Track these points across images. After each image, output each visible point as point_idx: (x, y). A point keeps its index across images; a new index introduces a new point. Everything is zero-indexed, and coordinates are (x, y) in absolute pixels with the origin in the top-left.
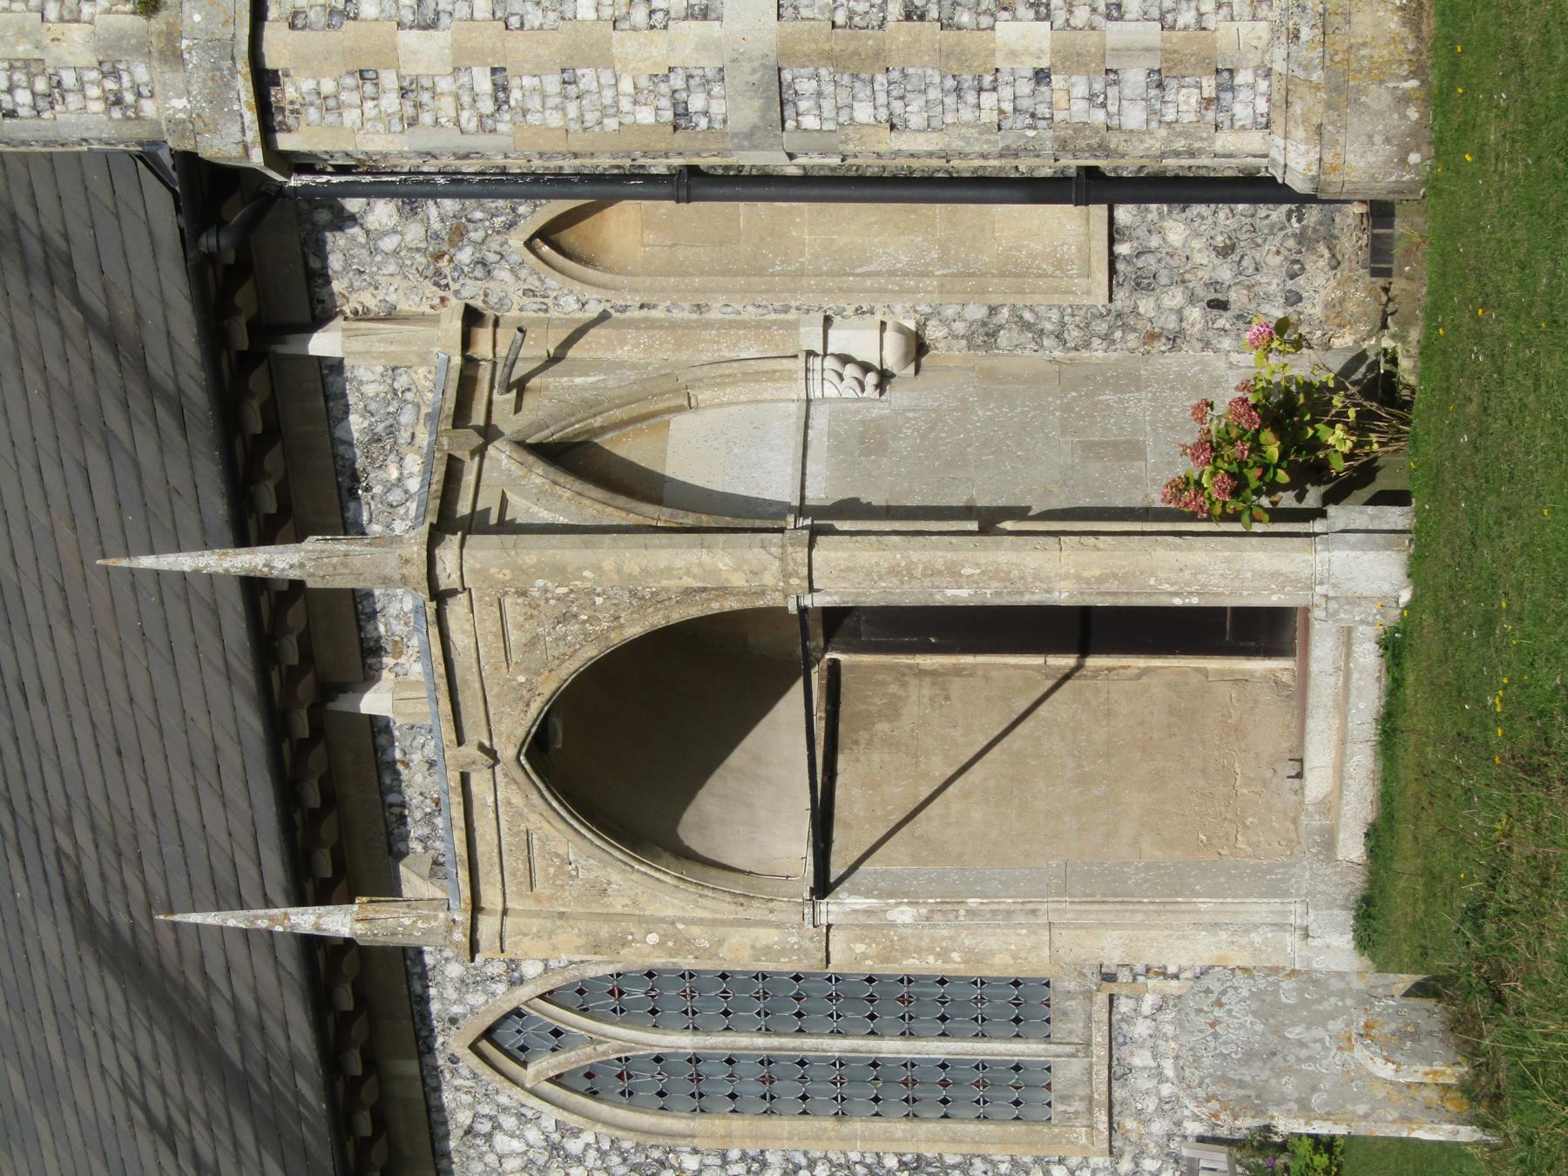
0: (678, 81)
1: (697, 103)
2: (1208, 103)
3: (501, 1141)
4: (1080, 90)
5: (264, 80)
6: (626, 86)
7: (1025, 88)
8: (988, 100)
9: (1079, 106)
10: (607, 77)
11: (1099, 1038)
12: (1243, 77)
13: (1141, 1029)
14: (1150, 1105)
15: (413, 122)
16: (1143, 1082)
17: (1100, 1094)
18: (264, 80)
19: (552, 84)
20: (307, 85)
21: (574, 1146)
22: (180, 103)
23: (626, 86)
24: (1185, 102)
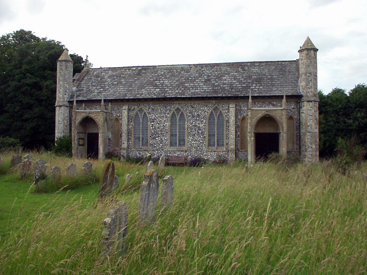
1: (309, 127)
12: (312, 160)
14: (212, 153)
15: (308, 110)
19: (311, 118)
23: (311, 123)
24: (310, 156)
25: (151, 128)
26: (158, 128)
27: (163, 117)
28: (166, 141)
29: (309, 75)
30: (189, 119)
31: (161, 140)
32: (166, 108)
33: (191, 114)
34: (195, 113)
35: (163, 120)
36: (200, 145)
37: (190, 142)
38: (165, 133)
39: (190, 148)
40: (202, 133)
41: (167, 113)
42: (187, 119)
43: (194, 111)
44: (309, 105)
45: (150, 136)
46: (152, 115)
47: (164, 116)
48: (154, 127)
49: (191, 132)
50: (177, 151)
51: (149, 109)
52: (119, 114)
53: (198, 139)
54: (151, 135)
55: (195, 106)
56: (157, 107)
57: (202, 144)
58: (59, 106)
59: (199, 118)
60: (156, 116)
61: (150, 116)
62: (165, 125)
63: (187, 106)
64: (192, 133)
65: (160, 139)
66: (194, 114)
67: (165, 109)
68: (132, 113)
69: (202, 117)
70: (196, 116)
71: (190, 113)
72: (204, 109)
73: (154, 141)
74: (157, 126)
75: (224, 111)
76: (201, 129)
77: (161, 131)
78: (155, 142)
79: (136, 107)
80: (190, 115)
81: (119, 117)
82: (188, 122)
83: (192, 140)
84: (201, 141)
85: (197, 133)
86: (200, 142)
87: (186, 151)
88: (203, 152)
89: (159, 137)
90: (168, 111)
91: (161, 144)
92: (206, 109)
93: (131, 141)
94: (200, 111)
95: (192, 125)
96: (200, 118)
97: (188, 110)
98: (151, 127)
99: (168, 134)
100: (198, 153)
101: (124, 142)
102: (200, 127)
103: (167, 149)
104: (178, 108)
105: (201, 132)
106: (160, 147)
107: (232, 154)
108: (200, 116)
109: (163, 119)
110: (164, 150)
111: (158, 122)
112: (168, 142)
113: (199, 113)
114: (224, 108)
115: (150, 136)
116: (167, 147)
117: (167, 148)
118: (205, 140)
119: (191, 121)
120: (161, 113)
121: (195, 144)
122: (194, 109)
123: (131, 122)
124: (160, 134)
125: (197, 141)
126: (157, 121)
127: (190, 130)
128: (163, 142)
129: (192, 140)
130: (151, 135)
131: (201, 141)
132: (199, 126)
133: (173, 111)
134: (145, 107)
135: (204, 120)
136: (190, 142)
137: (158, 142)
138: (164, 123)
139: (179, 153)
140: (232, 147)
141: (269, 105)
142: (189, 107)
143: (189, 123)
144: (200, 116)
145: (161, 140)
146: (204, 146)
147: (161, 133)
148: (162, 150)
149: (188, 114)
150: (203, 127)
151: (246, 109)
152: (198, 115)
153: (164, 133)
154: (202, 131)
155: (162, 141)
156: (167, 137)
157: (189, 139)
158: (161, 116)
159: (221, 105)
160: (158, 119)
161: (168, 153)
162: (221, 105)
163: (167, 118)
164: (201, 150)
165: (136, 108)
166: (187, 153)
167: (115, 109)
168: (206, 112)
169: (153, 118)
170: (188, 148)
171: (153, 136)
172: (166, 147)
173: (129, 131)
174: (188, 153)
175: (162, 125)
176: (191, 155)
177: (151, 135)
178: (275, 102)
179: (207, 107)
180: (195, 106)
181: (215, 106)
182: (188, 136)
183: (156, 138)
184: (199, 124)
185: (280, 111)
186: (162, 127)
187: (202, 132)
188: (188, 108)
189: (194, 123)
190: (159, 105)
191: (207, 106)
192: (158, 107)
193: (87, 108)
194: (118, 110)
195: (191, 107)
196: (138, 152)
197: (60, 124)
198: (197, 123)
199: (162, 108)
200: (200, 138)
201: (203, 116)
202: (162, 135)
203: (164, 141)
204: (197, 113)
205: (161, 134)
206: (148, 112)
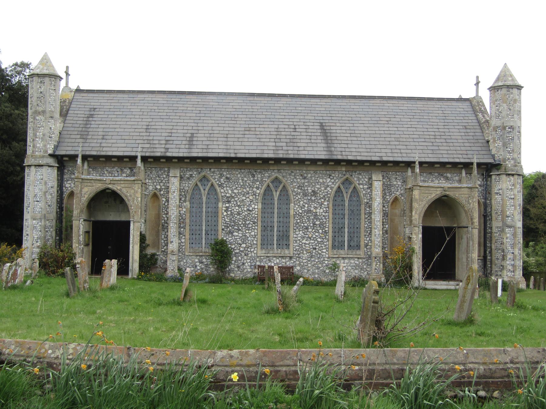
0: (512, 217)
1: (509, 218)
2: (510, 270)
4: (511, 257)
5: (513, 175)
6: (512, 211)
7: (511, 251)
8: (510, 248)
9: (509, 257)
10: (513, 209)
11: (349, 256)
12: (513, 273)
13: (353, 261)
16: (342, 261)
17: (340, 256)
18: (513, 175)
19: (512, 204)
20: (512, 179)
22: (509, 166)
23: (512, 211)
24: (510, 268)
26: (239, 214)
27: (248, 193)
28: (252, 239)
29: (509, 130)
30: (297, 198)
31: (243, 237)
32: (254, 177)
33: (301, 189)
34: (309, 188)
35: (248, 199)
36: (317, 247)
37: (298, 242)
38: (251, 223)
39: (298, 252)
40: (322, 225)
41: (255, 186)
42: (294, 199)
43: (306, 184)
44: (510, 181)
45: (223, 229)
46: (227, 190)
47: (250, 191)
48: (229, 213)
49: (300, 222)
50: (275, 257)
51: (221, 177)
52: (159, 185)
53: (314, 236)
54: (225, 226)
55: (309, 175)
56: (237, 174)
57: (321, 244)
58: (35, 166)
59: (315, 197)
60: (235, 191)
61: (222, 191)
62: (251, 209)
63: (293, 174)
64: (302, 225)
65: (241, 235)
66: (307, 190)
67: (252, 179)
68: (187, 185)
69: (321, 196)
70: (310, 194)
71: (298, 188)
72: (325, 181)
73: (230, 239)
74: (235, 210)
75: (361, 186)
76: (320, 217)
77: (245, 220)
78: (232, 241)
79: (195, 173)
80: (299, 191)
81: (160, 191)
82: (295, 204)
83: (303, 238)
84: (319, 240)
85: (311, 225)
86: (318, 241)
87: (291, 258)
88: (322, 259)
89: (240, 230)
90: (258, 183)
91: (244, 243)
92: (328, 181)
93: (183, 237)
94: (318, 185)
95: (303, 210)
96: (318, 198)
97: (295, 182)
98: (223, 211)
99: (257, 226)
101: (172, 240)
102: (318, 214)
103: (255, 253)
104: (276, 178)
105: (319, 222)
106: (241, 249)
107: (379, 264)
108: (318, 193)
109: (248, 198)
110: (250, 255)
111: (239, 204)
112: (257, 241)
113: (316, 189)
114: (361, 182)
115: (223, 229)
116: (256, 249)
117: (255, 252)
118: (327, 237)
119: (302, 203)
120: (243, 187)
121: (308, 244)
122: (306, 181)
123: (185, 201)
124: (242, 226)
125: (312, 239)
126: (236, 201)
127: (300, 219)
128: (248, 240)
129: (303, 238)
130: (223, 227)
131: (319, 240)
132: (317, 213)
133: (267, 183)
134: (212, 174)
135: (324, 202)
136: (299, 240)
137: (238, 240)
138: (250, 205)
139: (278, 261)
140: (377, 250)
141: (439, 179)
142: (298, 177)
143: (297, 206)
144: (318, 195)
145: (243, 237)
146: (324, 249)
147: (244, 222)
148: (246, 255)
149: (296, 190)
150: (323, 214)
151: (399, 183)
152: (313, 191)
153: (249, 224)
154: (321, 221)
155: (244, 239)
156: (256, 231)
157: (296, 235)
158: (243, 191)
159: (356, 176)
160: (239, 197)
161: (257, 261)
162: (356, 176)
163: (256, 196)
164: (318, 256)
165: (194, 175)
166: (293, 262)
167: (151, 176)
168: (328, 186)
169: (228, 195)
170: (296, 252)
171: (228, 229)
172: (252, 250)
173: (181, 218)
174: (295, 260)
175: (245, 209)
176: (299, 264)
177: (223, 227)
178: (450, 173)
179: (331, 177)
180: (309, 175)
181: (345, 177)
182: (295, 229)
183: (233, 232)
184: (316, 208)
185: (467, 190)
186: (246, 213)
188: (296, 178)
189: (306, 206)
190: (239, 171)
191: (330, 175)
192: (239, 176)
193: (92, 172)
194: (159, 177)
195: (301, 178)
196: (199, 259)
198: (312, 206)
199: (245, 177)
200: (317, 234)
201: (324, 194)
202: (245, 227)
203: (249, 239)
204: (313, 189)
205: (245, 225)
206: (218, 184)
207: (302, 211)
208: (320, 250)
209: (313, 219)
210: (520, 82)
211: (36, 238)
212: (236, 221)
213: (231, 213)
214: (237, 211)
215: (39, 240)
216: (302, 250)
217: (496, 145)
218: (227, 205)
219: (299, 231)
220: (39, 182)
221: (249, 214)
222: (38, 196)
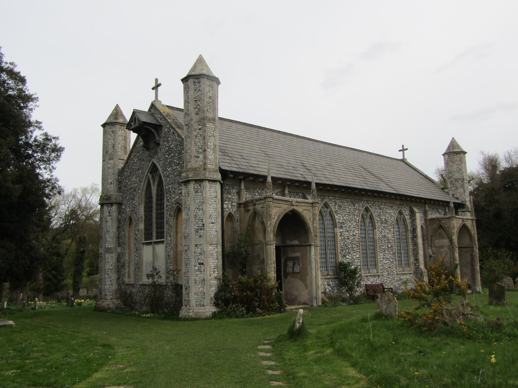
3: (392, 210)
13: (407, 277)
21: (392, 218)
25: (340, 238)
34: (383, 217)
35: (352, 225)
36: (391, 266)
38: (356, 246)
48: (343, 237)
50: (371, 276)
53: (389, 257)
54: (341, 250)
56: (345, 203)
58: (210, 181)
60: (345, 218)
67: (353, 207)
84: (391, 260)
95: (382, 235)
100: (390, 278)
109: (352, 224)
111: (348, 229)
112: (360, 262)
122: (381, 211)
128: (355, 262)
152: (385, 220)
171: (343, 252)
175: (352, 234)
184: (388, 233)
187: (392, 247)
196: (327, 282)
197: (213, 223)
200: (390, 255)
203: (356, 261)
207: (382, 236)
208: (392, 269)
209: (387, 243)
210: (465, 150)
211: (213, 268)
212: (347, 245)
213: (344, 237)
214: (347, 236)
215: (216, 270)
216: (384, 269)
217: (459, 191)
218: (341, 230)
219: (381, 253)
220: (213, 201)
221: (354, 238)
222: (213, 216)
